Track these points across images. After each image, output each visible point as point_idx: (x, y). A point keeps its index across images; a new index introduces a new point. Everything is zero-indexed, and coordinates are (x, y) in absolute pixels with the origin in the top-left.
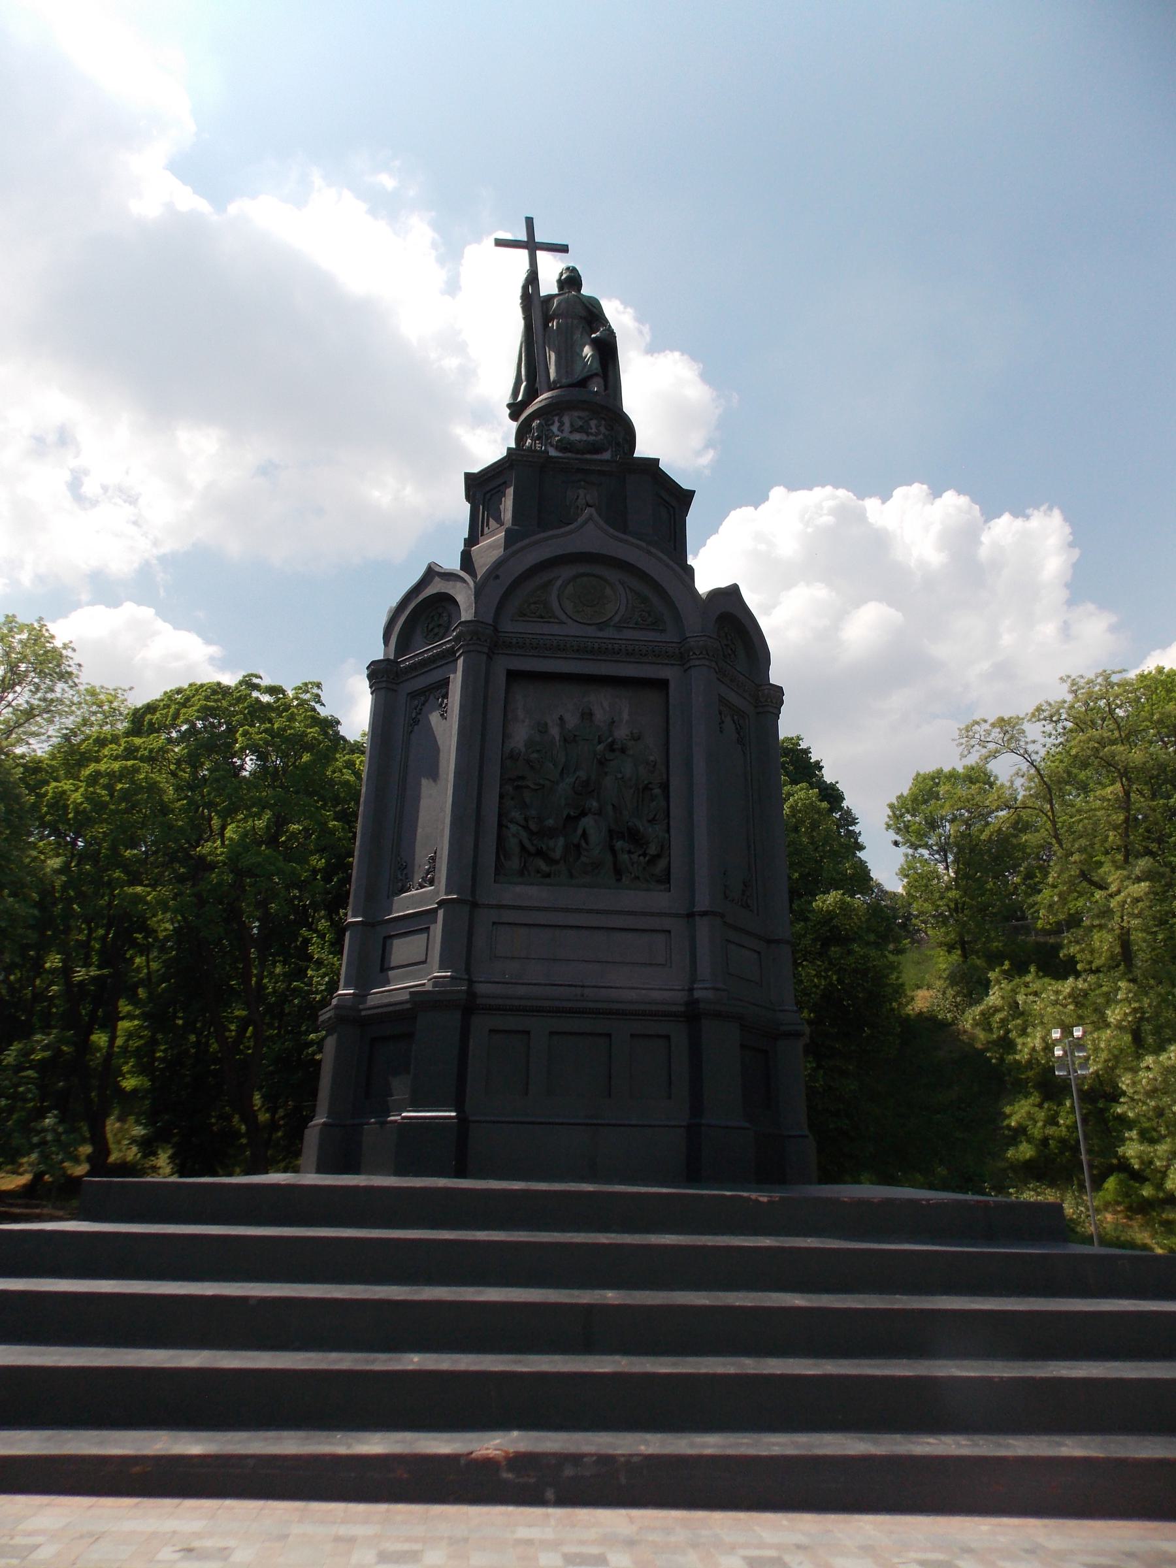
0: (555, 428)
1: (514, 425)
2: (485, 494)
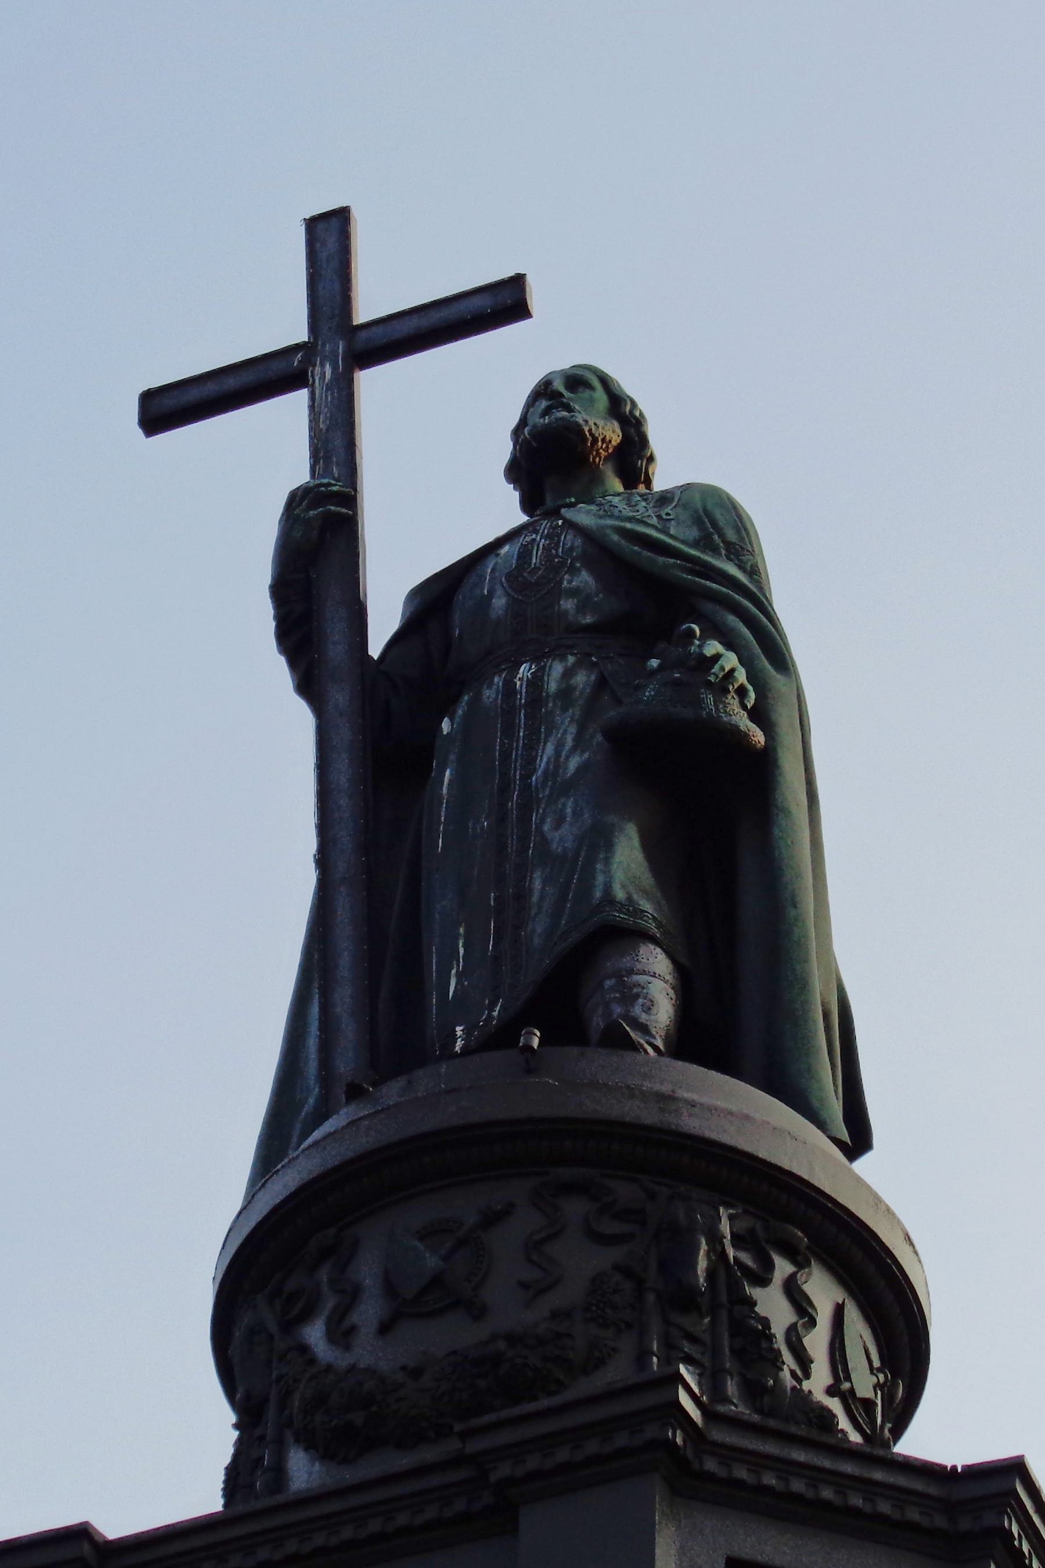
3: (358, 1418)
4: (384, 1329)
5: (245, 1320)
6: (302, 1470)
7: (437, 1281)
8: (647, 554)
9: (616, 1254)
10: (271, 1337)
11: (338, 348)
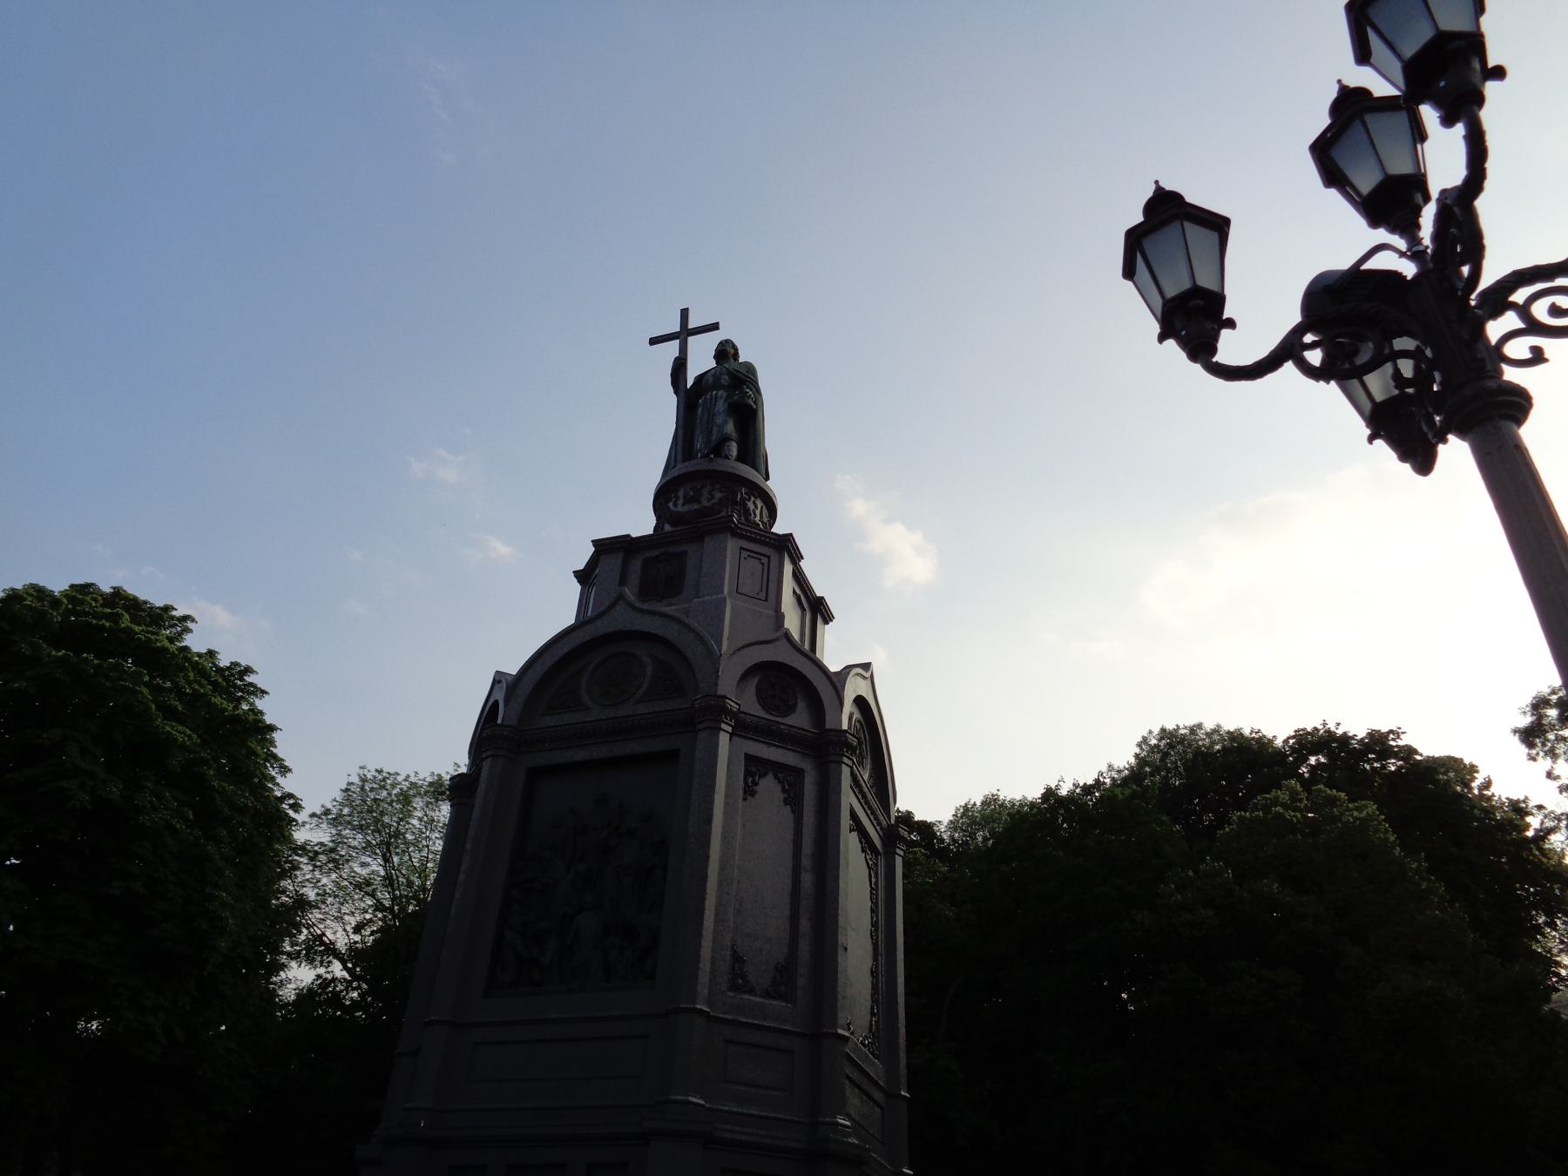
0: (671, 505)
6: (667, 528)
11: (684, 333)
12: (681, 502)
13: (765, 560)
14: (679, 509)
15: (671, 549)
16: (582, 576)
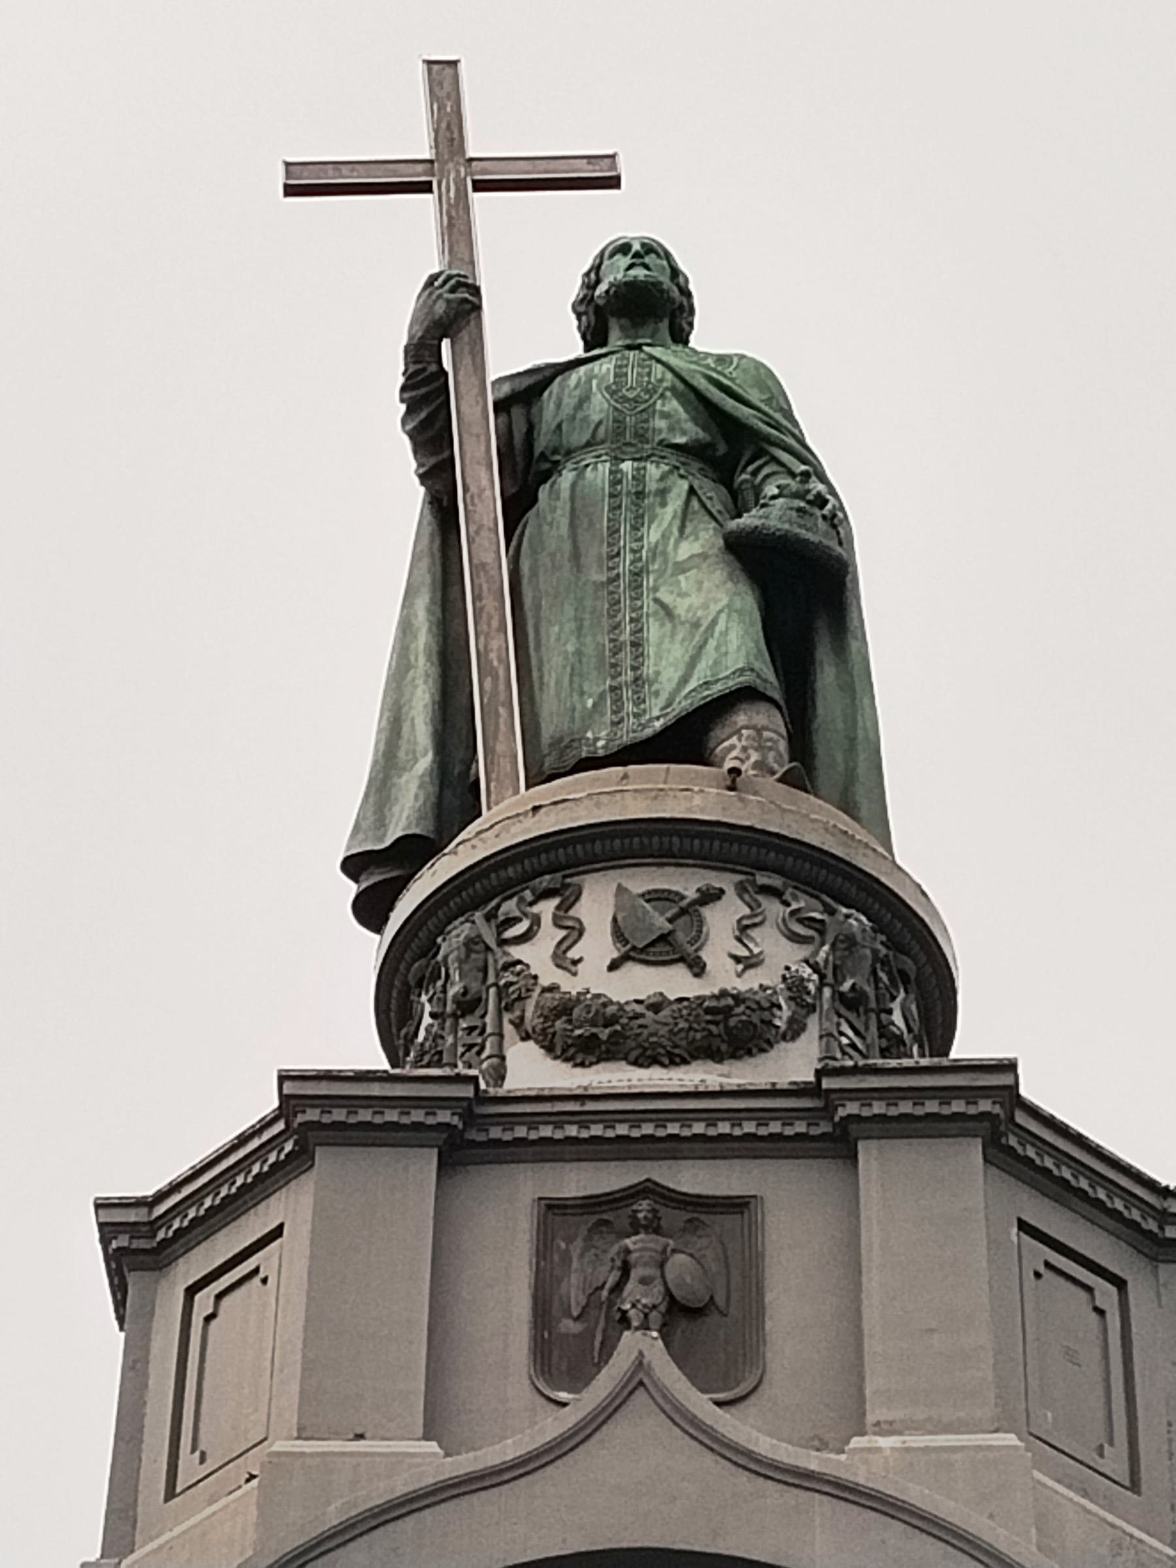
1: (370, 948)
2: (192, 1291)
3: (604, 1034)
4: (614, 966)
5: (460, 931)
7: (663, 938)
8: (731, 401)
9: (804, 951)
10: (488, 948)
11: (451, 173)
12: (597, 946)
13: (1106, 1293)
14: (599, 974)
15: (691, 1178)
16: (140, 1243)
